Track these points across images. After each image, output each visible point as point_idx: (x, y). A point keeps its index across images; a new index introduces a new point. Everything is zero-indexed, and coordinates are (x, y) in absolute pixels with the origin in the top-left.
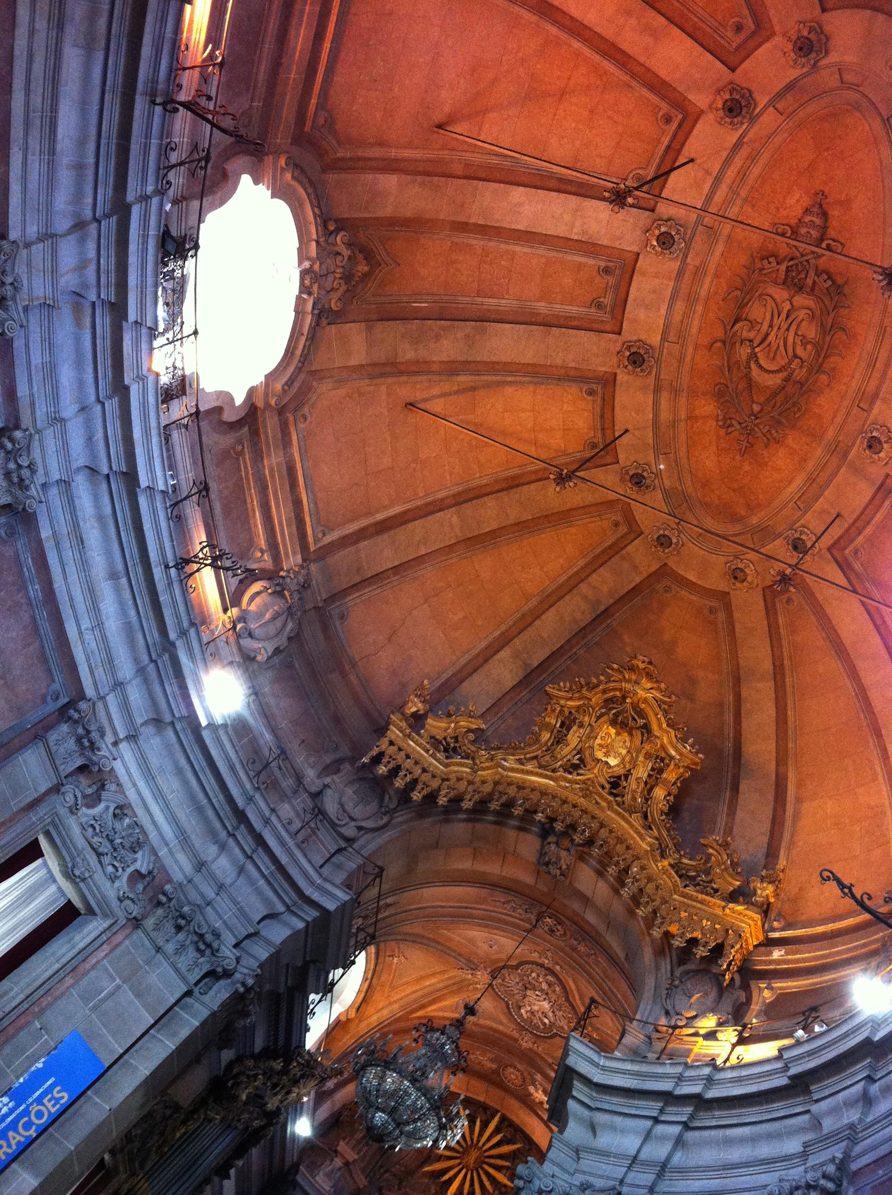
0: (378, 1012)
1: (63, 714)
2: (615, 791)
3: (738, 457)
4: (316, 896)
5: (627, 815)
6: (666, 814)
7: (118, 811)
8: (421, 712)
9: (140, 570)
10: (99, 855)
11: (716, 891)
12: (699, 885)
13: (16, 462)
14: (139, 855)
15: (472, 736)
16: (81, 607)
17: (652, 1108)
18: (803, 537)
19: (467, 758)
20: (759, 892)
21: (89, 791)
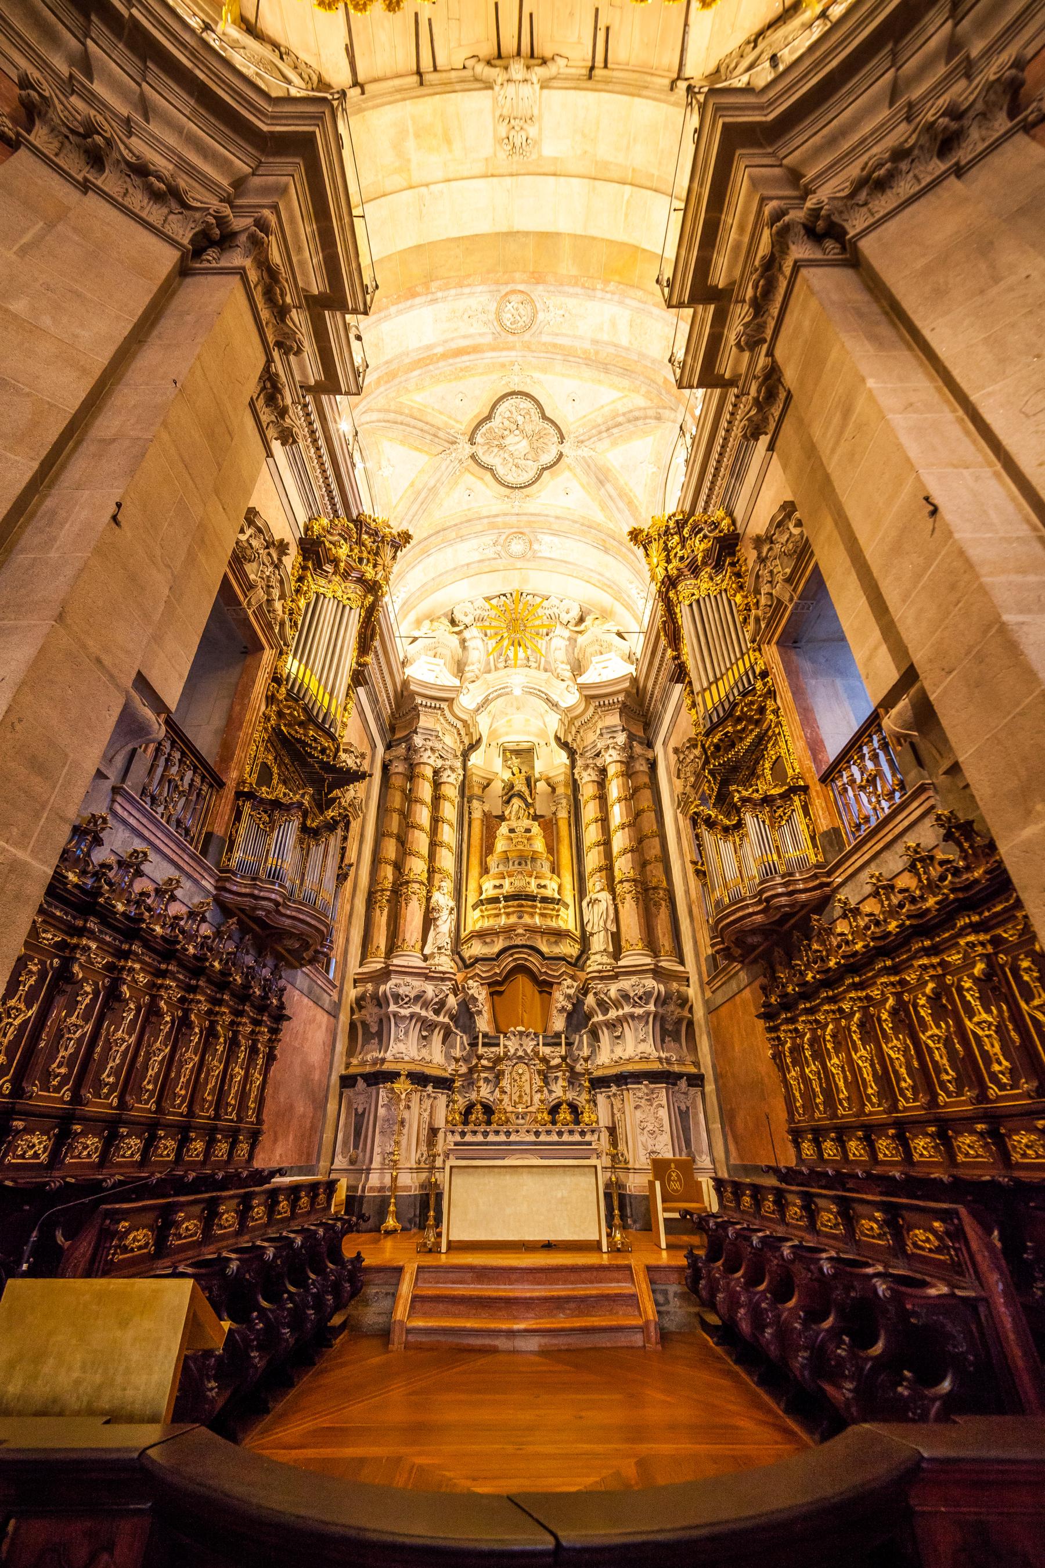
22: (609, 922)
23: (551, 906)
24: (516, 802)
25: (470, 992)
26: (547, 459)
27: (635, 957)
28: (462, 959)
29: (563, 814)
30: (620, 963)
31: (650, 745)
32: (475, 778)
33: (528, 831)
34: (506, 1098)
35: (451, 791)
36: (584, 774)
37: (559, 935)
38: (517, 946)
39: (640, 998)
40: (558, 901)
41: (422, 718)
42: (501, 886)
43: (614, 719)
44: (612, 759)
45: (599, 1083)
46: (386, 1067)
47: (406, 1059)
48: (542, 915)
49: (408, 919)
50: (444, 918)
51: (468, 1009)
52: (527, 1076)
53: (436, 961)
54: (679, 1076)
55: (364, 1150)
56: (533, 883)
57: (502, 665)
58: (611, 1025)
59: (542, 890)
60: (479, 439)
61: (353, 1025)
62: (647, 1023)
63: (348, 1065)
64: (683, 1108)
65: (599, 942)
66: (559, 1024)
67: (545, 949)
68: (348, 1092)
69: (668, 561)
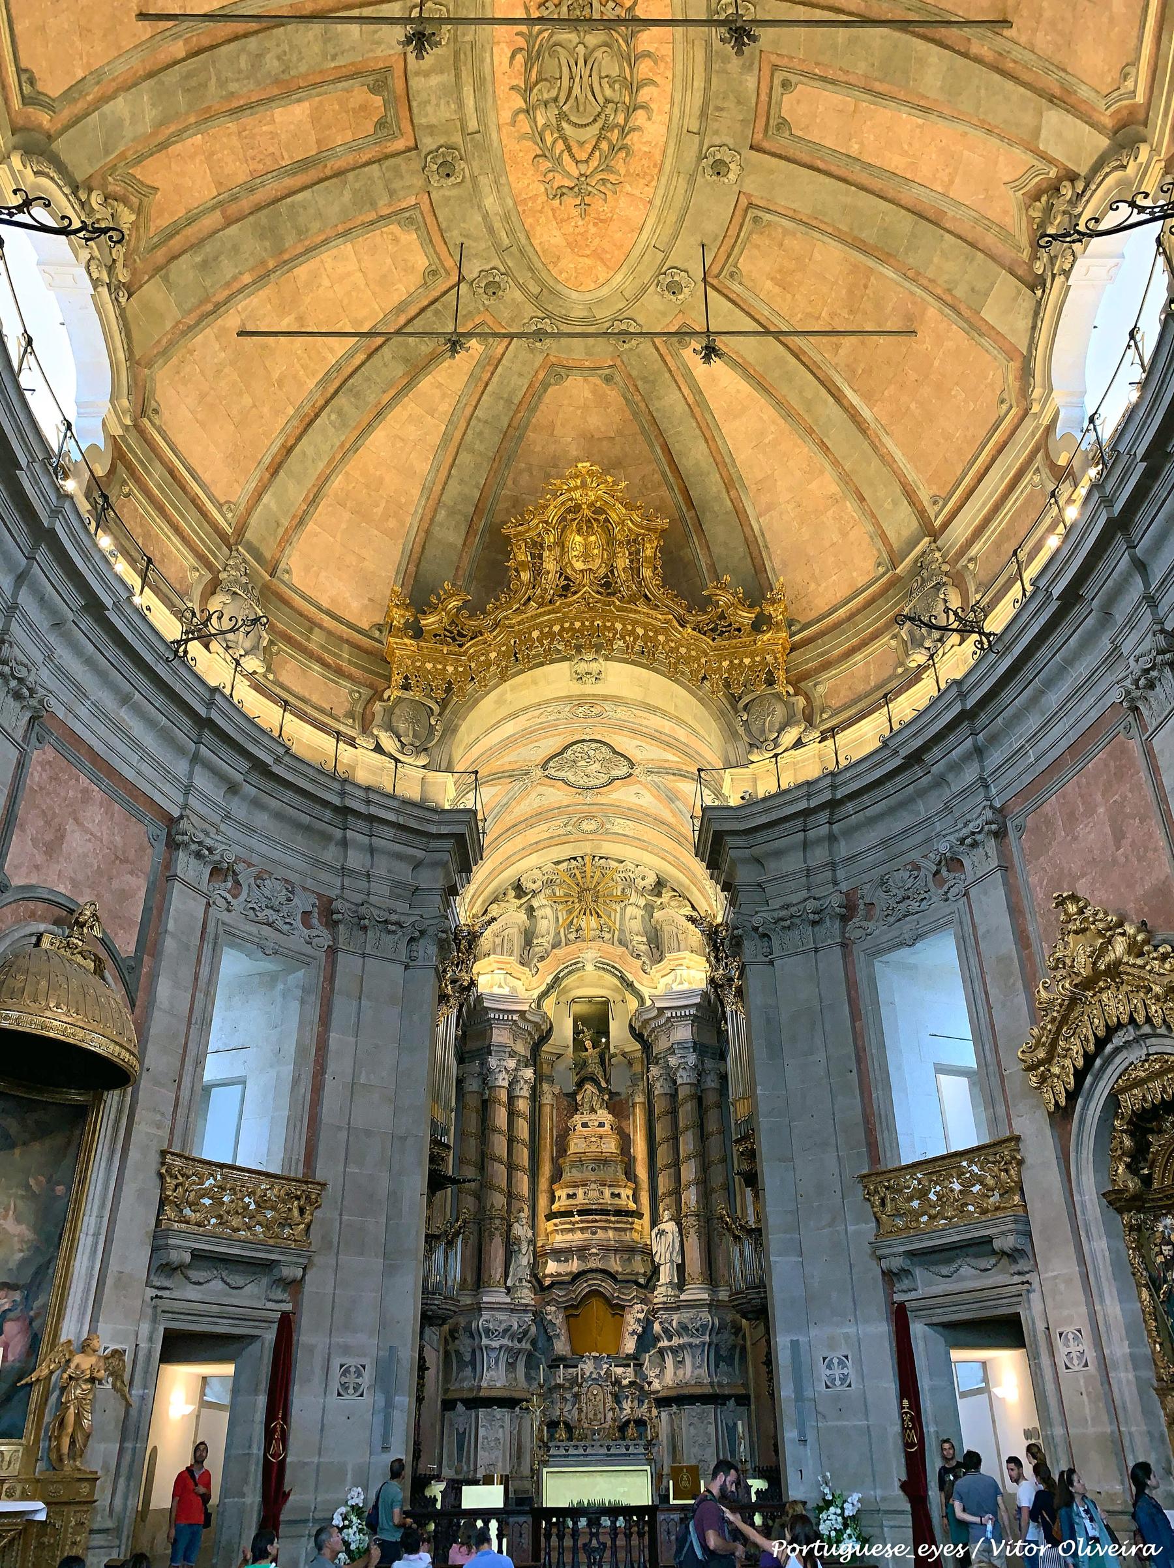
1: (173, 845)
3: (580, 223)
4: (444, 830)
5: (634, 607)
7: (259, 882)
9: (141, 676)
10: (270, 925)
11: (739, 630)
12: (723, 632)
13: (15, 678)
14: (296, 901)
15: (466, 613)
16: (122, 748)
18: (676, 278)
19: (476, 637)
20: (774, 615)
21: (229, 885)
22: (675, 1254)
23: (625, 1219)
24: (589, 1087)
25: (549, 1317)
26: (616, 773)
27: (695, 1293)
28: (539, 1282)
29: (640, 1098)
31: (722, 1056)
32: (543, 1055)
33: (601, 1125)
35: (523, 1105)
36: (658, 1085)
37: (630, 1251)
38: (592, 1271)
39: (697, 1330)
41: (495, 1031)
42: (575, 1194)
43: (683, 1033)
44: (683, 1077)
45: (663, 1402)
46: (482, 1394)
47: (498, 1385)
48: (615, 1229)
50: (524, 1251)
51: (546, 1331)
52: (601, 1396)
54: (728, 1397)
56: (607, 1192)
58: (674, 1351)
59: (616, 1201)
60: (551, 764)
61: (447, 1354)
62: (703, 1351)
63: (446, 1391)
65: (666, 1275)
66: (630, 1346)
67: (615, 1265)
68: (448, 1414)
69: (718, 960)
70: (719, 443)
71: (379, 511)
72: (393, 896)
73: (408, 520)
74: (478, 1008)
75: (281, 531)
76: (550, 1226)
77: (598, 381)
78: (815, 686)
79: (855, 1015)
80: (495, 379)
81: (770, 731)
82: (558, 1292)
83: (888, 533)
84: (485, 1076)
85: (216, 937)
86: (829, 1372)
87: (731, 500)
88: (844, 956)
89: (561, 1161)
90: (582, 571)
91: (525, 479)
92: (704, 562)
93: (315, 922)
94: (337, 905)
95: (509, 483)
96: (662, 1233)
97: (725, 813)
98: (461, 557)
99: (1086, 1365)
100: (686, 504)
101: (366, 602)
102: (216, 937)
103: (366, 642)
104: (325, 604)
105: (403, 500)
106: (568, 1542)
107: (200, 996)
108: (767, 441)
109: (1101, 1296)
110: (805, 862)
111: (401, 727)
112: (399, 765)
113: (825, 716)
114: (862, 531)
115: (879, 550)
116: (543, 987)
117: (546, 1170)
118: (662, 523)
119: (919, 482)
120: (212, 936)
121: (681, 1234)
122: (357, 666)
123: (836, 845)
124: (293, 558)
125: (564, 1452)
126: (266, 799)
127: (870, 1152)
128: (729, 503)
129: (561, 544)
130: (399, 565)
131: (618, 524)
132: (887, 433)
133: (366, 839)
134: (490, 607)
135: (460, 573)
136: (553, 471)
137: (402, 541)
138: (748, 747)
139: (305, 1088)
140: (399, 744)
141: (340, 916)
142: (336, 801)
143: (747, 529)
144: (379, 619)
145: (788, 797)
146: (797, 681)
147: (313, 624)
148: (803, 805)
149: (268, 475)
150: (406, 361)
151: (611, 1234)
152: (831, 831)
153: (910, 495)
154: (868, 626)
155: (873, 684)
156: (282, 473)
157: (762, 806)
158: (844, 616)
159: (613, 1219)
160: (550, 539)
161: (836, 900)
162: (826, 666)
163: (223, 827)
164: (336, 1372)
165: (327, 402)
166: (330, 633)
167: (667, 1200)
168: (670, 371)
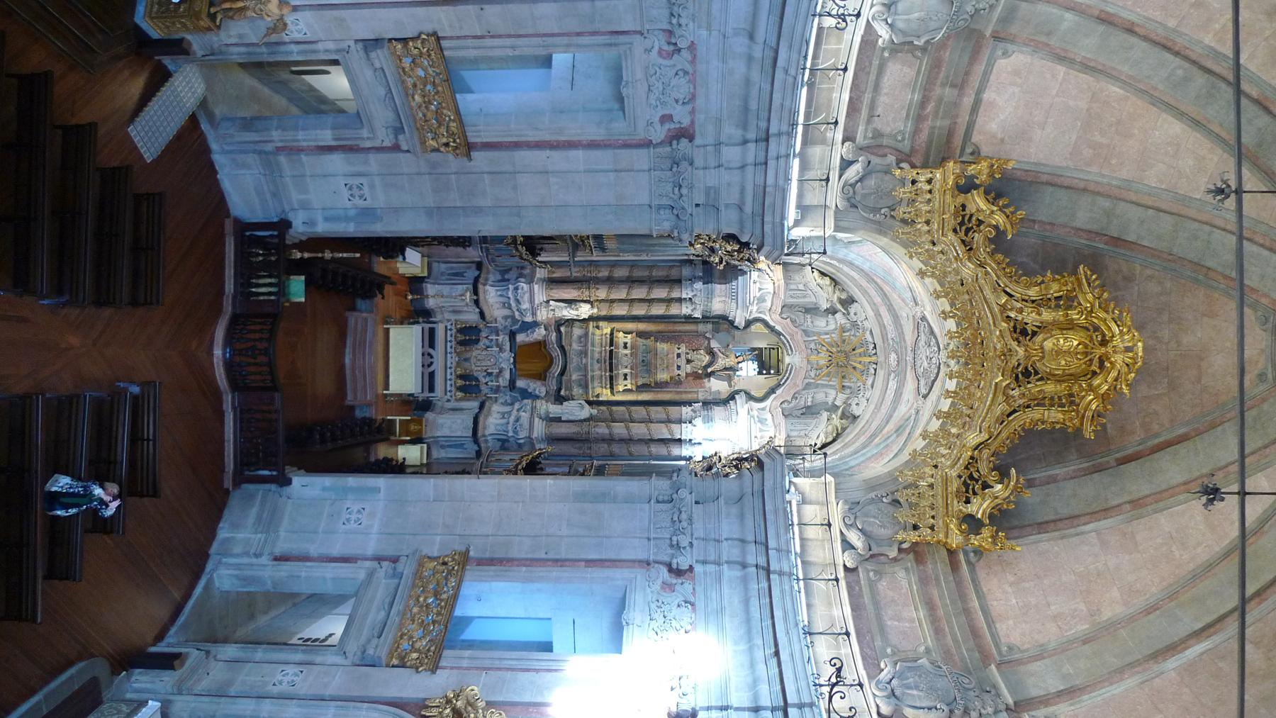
0: (858, 255)
2: (1020, 375)
4: (767, 228)
6: (1023, 429)
7: (681, 73)
8: (977, 182)
14: (679, 108)
17: (761, 538)
23: (608, 383)
24: (707, 359)
26: (922, 382)
27: (539, 429)
30: (537, 420)
33: (679, 367)
34: (479, 352)
35: (674, 310)
36: (690, 408)
40: (612, 388)
41: (723, 286)
48: (602, 376)
49: (566, 290)
50: (571, 312)
53: (543, 309)
54: (479, 446)
55: (447, 280)
57: (812, 346)
58: (510, 413)
64: (465, 446)
65: (555, 409)
66: (521, 383)
68: (474, 266)
70: (1181, 497)
71: (1098, 138)
72: (708, 191)
73: (1094, 169)
74: (739, 272)
75: (1043, 39)
76: (608, 331)
77: (1260, 366)
78: (907, 570)
79: (590, 563)
80: (1255, 248)
81: (864, 522)
82: (554, 336)
83: (1039, 663)
84: (692, 279)
85: (616, 45)
86: (355, 511)
87: (1118, 506)
88: (640, 561)
89: (652, 338)
90: (1042, 348)
91: (1153, 287)
92: (1058, 471)
93: (667, 126)
94: (684, 142)
95: (1149, 272)
96: (582, 407)
97: (779, 475)
98: (1065, 226)
99: (274, 685)
100: (1124, 458)
101: (999, 136)
102: (616, 45)
103: (958, 141)
104: (987, 96)
105: (1113, 162)
106: (257, 336)
107: (565, 40)
108: (1174, 548)
109: (299, 706)
110: (726, 539)
111: (872, 182)
112: (824, 183)
113: (871, 574)
114: (1051, 634)
115: (1027, 650)
116: (772, 323)
117: (642, 326)
118: (1089, 431)
119: (1078, 706)
120: (617, 41)
121: (581, 421)
122: (931, 134)
123: (739, 567)
124: (1021, 57)
125: (449, 339)
126: (756, 68)
127: (487, 559)
128: (1115, 502)
129: (1070, 326)
130: (1043, 165)
131: (1090, 385)
132: (1143, 682)
133: (750, 159)
134: (1000, 257)
135: (1048, 227)
136: (1165, 317)
137: (1070, 164)
138: (857, 500)
139: (532, 136)
140: (852, 181)
141: (674, 146)
142: (773, 130)
143: (1086, 518)
144: (985, 150)
145: (782, 531)
146: (917, 552)
147: (961, 86)
148: (772, 544)
149: (1096, 13)
150: (1259, 145)
151: (597, 373)
152: (751, 566)
153: (1070, 693)
154: (951, 628)
155: (889, 623)
156: (1102, 28)
157: (781, 507)
158: (971, 605)
159: (607, 374)
160: (1074, 314)
161: (683, 562)
162: (924, 581)
163: (714, 33)
164: (355, 181)
165: (1194, 62)
166: (956, 105)
167: (607, 414)
168: (1266, 447)
